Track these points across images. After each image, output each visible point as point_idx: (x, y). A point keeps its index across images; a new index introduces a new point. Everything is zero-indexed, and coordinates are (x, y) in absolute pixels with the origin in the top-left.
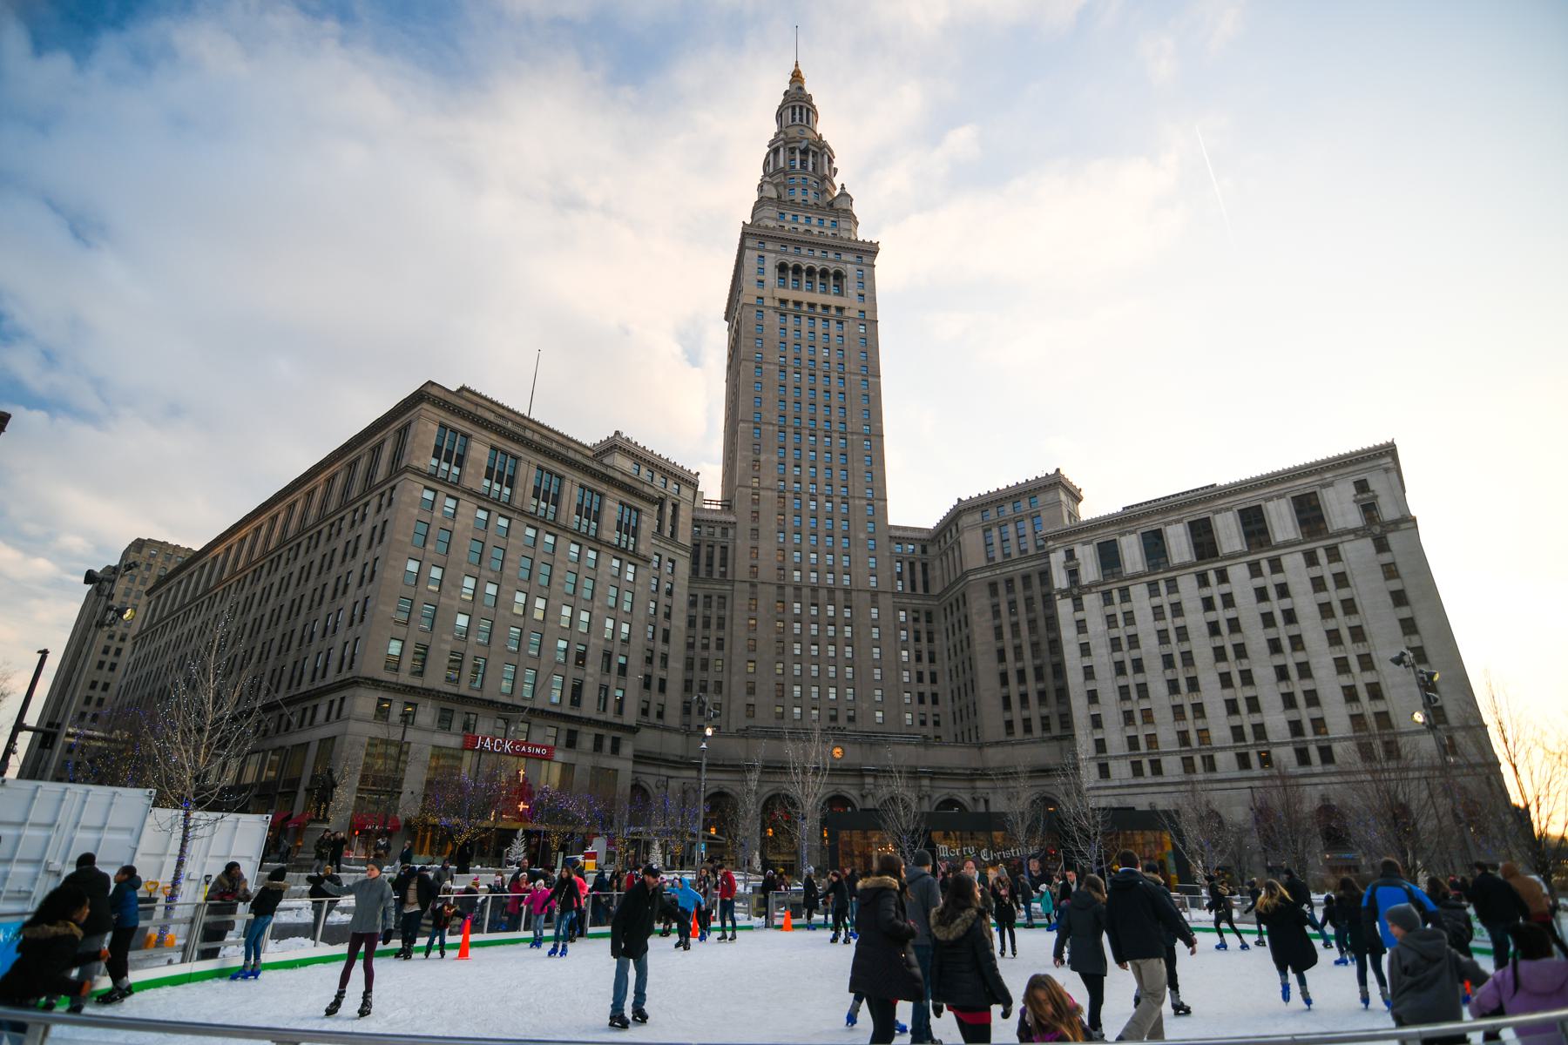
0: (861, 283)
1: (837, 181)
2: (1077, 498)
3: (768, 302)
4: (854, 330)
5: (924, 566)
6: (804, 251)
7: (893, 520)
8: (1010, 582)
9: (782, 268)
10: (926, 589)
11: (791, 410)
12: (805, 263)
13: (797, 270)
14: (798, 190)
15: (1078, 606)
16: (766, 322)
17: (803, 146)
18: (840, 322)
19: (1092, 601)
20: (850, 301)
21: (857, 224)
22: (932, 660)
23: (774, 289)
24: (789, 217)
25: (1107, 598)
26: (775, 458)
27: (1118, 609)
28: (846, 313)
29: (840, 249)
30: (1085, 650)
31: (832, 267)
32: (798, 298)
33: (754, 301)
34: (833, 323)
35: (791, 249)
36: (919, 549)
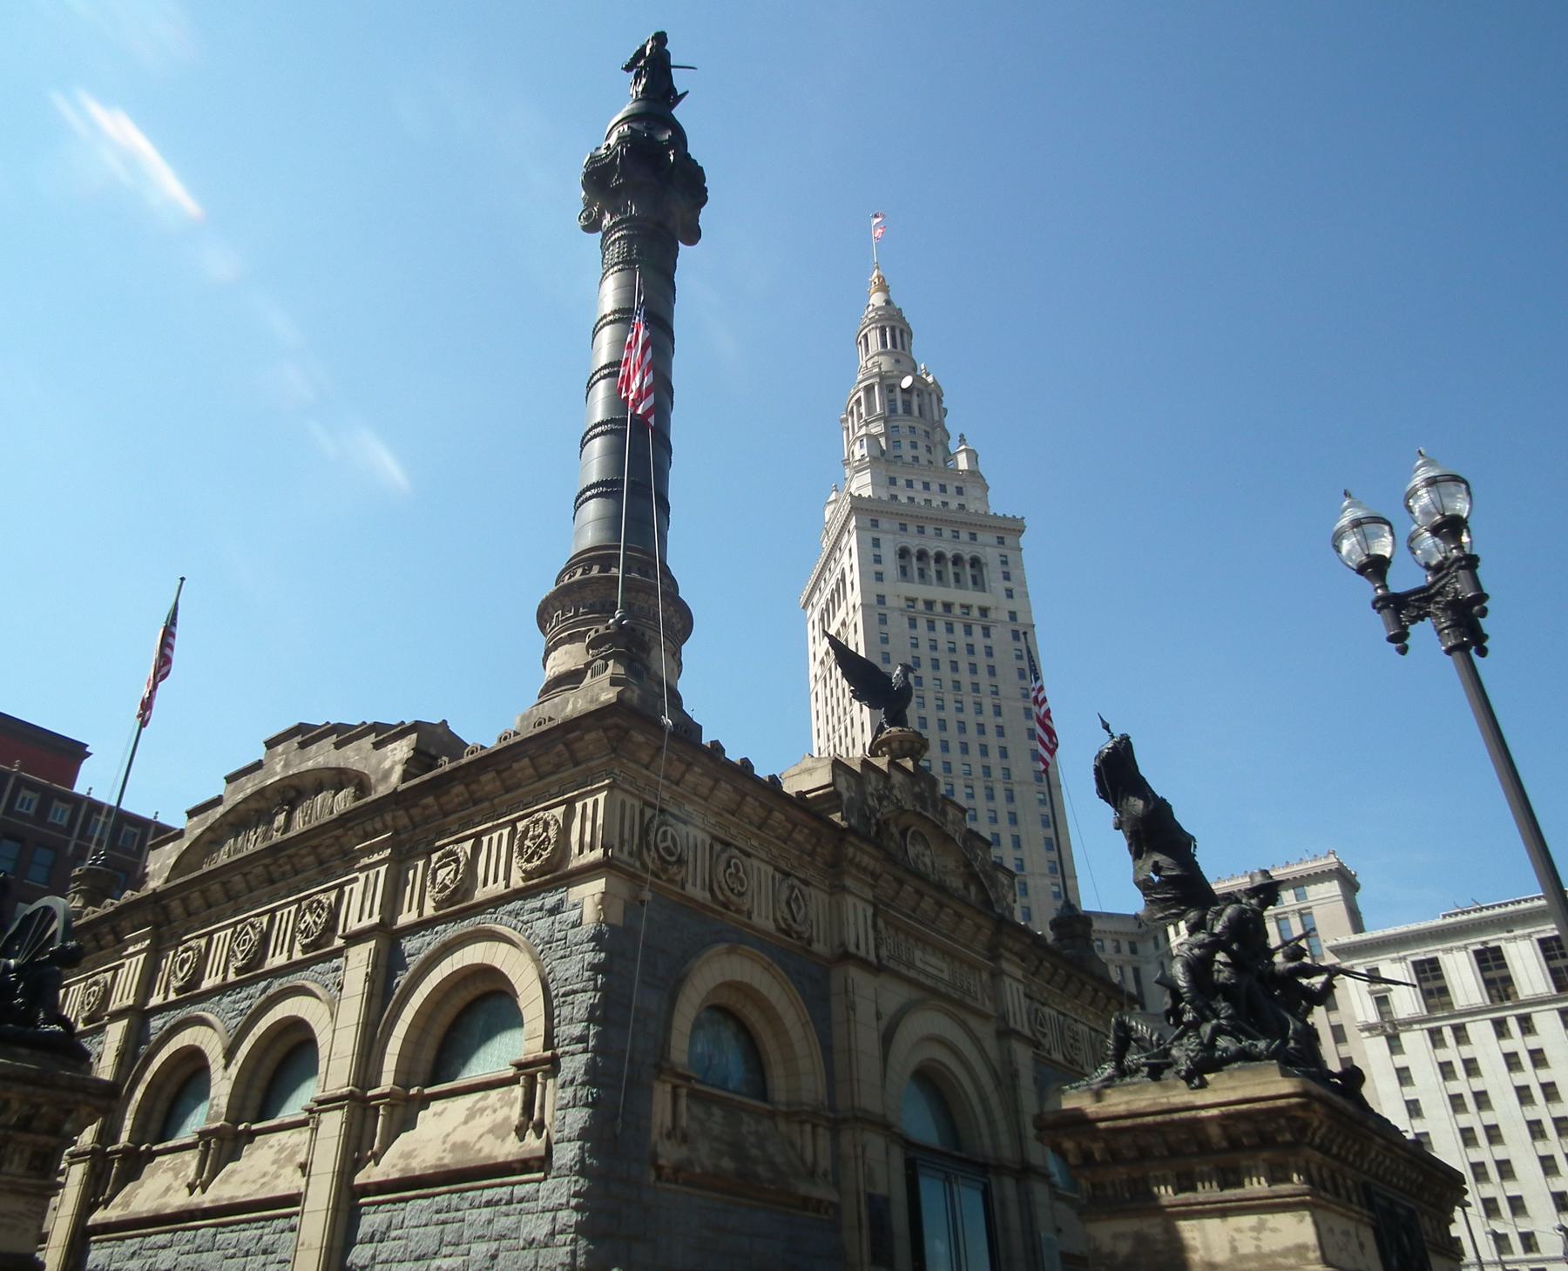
0: (1007, 577)
2: (1350, 884)
3: (889, 601)
4: (1001, 636)
5: (1136, 971)
6: (930, 530)
9: (903, 553)
12: (933, 547)
13: (922, 555)
14: (906, 445)
15: (1394, 1045)
17: (907, 382)
18: (986, 632)
19: (1415, 1042)
20: (993, 597)
21: (987, 488)
23: (897, 590)
24: (901, 482)
25: (1436, 1038)
28: (992, 615)
31: (967, 552)
32: (930, 597)
33: (874, 600)
34: (977, 631)
35: (912, 528)
36: (1125, 947)
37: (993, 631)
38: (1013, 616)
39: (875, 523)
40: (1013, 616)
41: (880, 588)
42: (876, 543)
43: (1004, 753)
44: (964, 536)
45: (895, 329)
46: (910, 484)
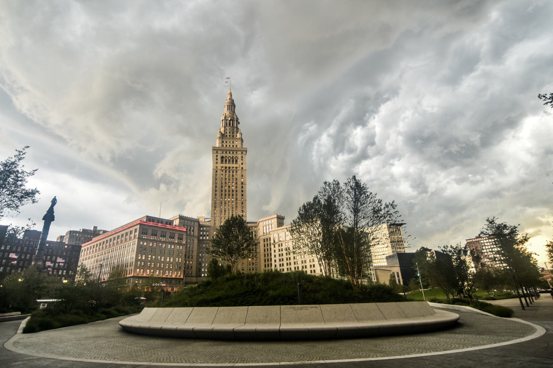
1: (239, 126)
5: (255, 232)
6: (228, 152)
8: (267, 239)
9: (222, 157)
11: (223, 196)
16: (218, 173)
17: (229, 119)
19: (277, 246)
23: (220, 165)
24: (225, 142)
27: (280, 248)
29: (237, 151)
30: (275, 256)
31: (235, 156)
33: (215, 168)
35: (224, 152)
38: (242, 168)
39: (217, 152)
40: (242, 168)
42: (217, 156)
44: (235, 153)
45: (232, 105)
46: (226, 142)
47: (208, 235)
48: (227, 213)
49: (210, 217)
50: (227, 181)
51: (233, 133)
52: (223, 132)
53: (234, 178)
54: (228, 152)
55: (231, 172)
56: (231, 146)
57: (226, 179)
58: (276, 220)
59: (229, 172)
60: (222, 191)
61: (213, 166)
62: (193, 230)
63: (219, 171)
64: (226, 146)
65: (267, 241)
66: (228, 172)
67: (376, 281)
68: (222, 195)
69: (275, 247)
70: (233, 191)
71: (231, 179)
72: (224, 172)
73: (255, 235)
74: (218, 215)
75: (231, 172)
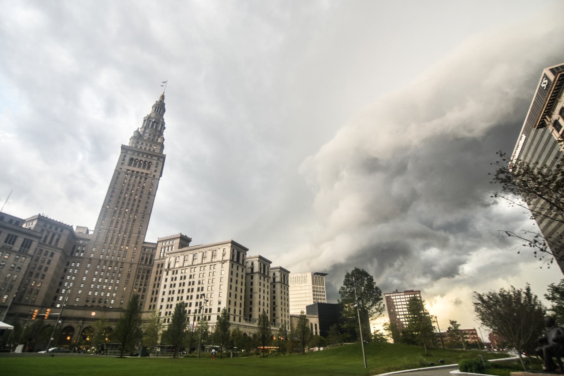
3: (123, 170)
6: (141, 155)
7: (146, 241)
9: (132, 159)
10: (150, 263)
12: (139, 159)
16: (121, 176)
17: (154, 120)
18: (146, 179)
19: (170, 272)
22: (145, 285)
23: (126, 167)
24: (140, 143)
26: (111, 220)
29: (152, 156)
31: (148, 160)
35: (136, 154)
37: (148, 179)
38: (154, 176)
39: (126, 152)
41: (122, 167)
42: (125, 156)
43: (138, 206)
44: (149, 157)
46: (142, 144)
47: (83, 252)
48: (119, 226)
49: (93, 229)
50: (131, 187)
51: (154, 136)
52: (141, 133)
53: (141, 185)
54: (141, 155)
55: (139, 178)
56: (147, 149)
57: (129, 185)
58: (178, 241)
59: (136, 177)
60: (120, 198)
61: (117, 167)
62: (58, 240)
63: (122, 174)
64: (141, 147)
65: (162, 266)
66: (134, 177)
67: (290, 330)
68: (118, 202)
69: (167, 274)
70: (135, 200)
71: (136, 186)
72: (129, 176)
73: (151, 259)
74: (105, 227)
75: (139, 178)
